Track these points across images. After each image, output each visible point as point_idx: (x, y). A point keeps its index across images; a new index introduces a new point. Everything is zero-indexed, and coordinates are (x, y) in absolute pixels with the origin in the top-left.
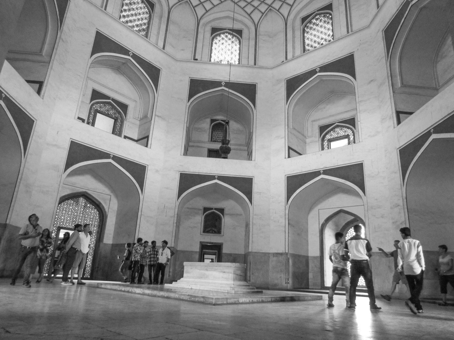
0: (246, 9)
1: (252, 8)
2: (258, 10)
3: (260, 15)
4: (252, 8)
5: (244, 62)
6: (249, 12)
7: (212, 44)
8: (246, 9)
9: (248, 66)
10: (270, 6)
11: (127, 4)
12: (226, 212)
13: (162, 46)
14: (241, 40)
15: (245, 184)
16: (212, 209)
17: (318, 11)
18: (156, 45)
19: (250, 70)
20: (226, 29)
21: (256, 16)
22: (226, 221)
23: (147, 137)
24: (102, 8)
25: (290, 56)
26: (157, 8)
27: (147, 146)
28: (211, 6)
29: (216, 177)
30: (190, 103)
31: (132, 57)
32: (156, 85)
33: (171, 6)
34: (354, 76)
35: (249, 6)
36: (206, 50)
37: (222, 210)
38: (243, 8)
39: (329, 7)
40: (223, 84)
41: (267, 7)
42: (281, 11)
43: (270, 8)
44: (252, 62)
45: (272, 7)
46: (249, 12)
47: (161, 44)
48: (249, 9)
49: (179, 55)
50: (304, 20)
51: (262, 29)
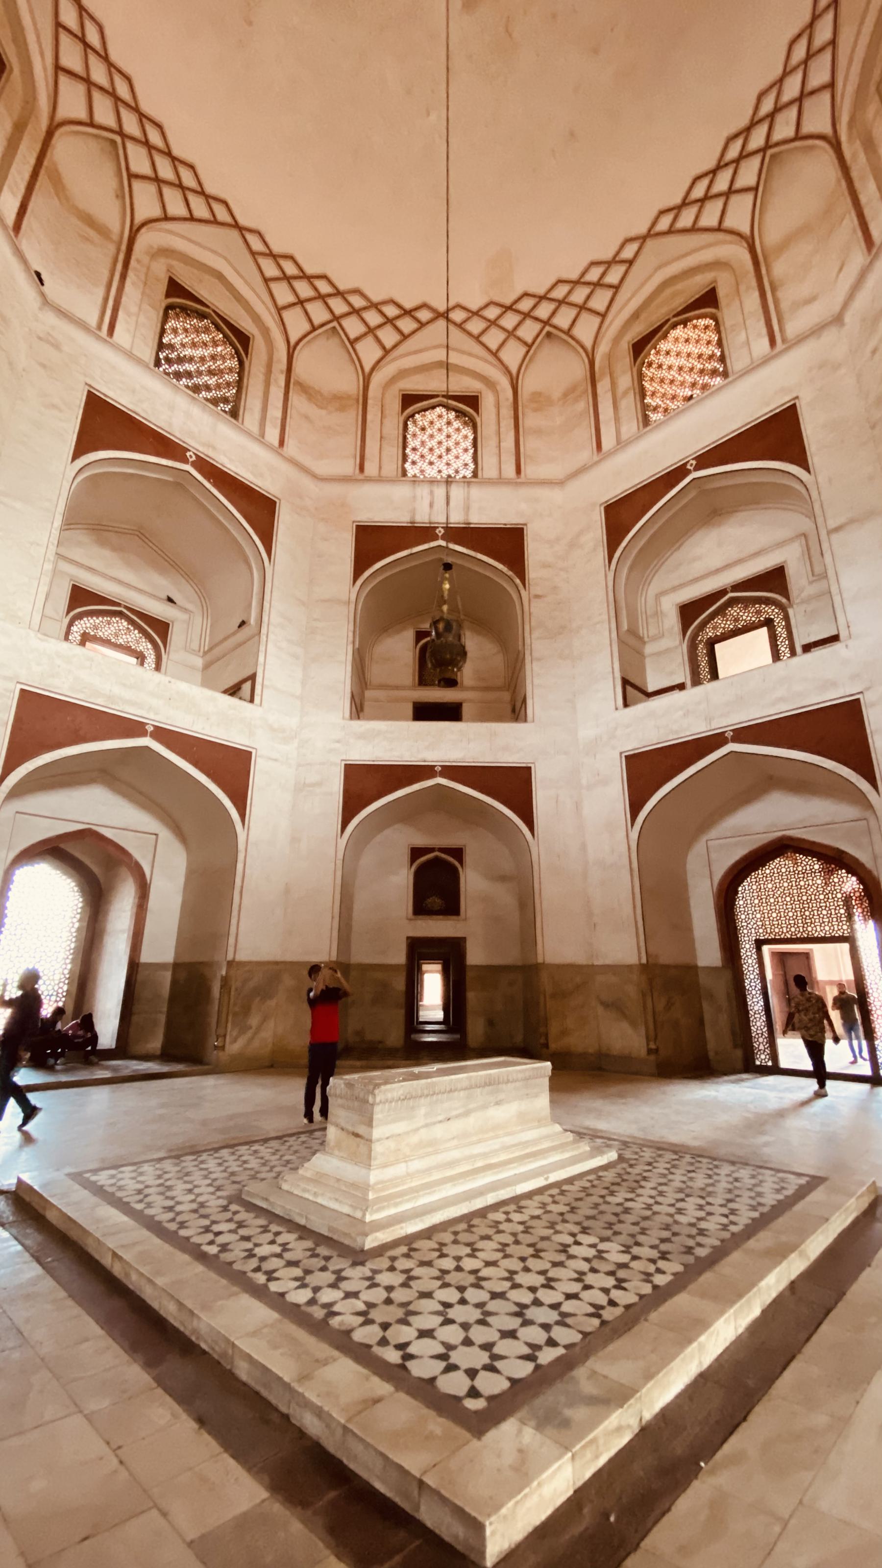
0: (484, 339)
1: (502, 336)
2: (519, 339)
3: (524, 349)
4: (502, 336)
5: (489, 470)
6: (494, 347)
7: (405, 438)
8: (484, 339)
9: (500, 481)
10: (546, 323)
11: (175, 331)
12: (468, 858)
13: (276, 442)
14: (478, 420)
15: (513, 786)
16: (432, 850)
17: (675, 316)
18: (260, 438)
19: (505, 492)
20: (437, 396)
21: (512, 355)
22: (472, 882)
23: (253, 678)
24: (99, 327)
25: (608, 442)
26: (258, 345)
27: (252, 701)
28: (397, 337)
29: (438, 769)
30: (359, 582)
31: (194, 464)
32: (267, 539)
33: (293, 341)
34: (801, 460)
35: (494, 331)
36: (392, 451)
37: (458, 853)
38: (477, 338)
39: (709, 299)
40: (440, 532)
41: (538, 326)
42: (576, 332)
43: (548, 328)
44: (509, 470)
45: (551, 325)
46: (494, 347)
47: (272, 435)
48: (493, 339)
49: (323, 468)
50: (639, 348)
51: (529, 384)
